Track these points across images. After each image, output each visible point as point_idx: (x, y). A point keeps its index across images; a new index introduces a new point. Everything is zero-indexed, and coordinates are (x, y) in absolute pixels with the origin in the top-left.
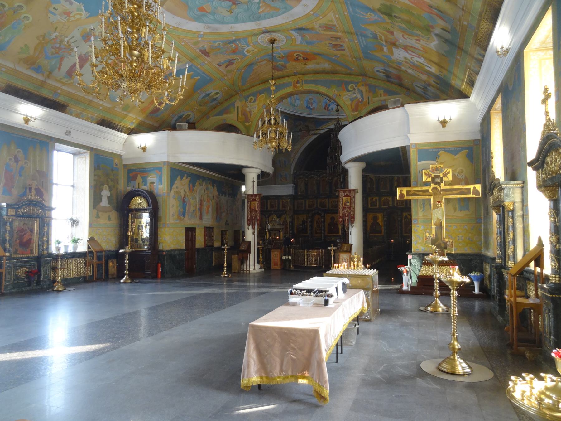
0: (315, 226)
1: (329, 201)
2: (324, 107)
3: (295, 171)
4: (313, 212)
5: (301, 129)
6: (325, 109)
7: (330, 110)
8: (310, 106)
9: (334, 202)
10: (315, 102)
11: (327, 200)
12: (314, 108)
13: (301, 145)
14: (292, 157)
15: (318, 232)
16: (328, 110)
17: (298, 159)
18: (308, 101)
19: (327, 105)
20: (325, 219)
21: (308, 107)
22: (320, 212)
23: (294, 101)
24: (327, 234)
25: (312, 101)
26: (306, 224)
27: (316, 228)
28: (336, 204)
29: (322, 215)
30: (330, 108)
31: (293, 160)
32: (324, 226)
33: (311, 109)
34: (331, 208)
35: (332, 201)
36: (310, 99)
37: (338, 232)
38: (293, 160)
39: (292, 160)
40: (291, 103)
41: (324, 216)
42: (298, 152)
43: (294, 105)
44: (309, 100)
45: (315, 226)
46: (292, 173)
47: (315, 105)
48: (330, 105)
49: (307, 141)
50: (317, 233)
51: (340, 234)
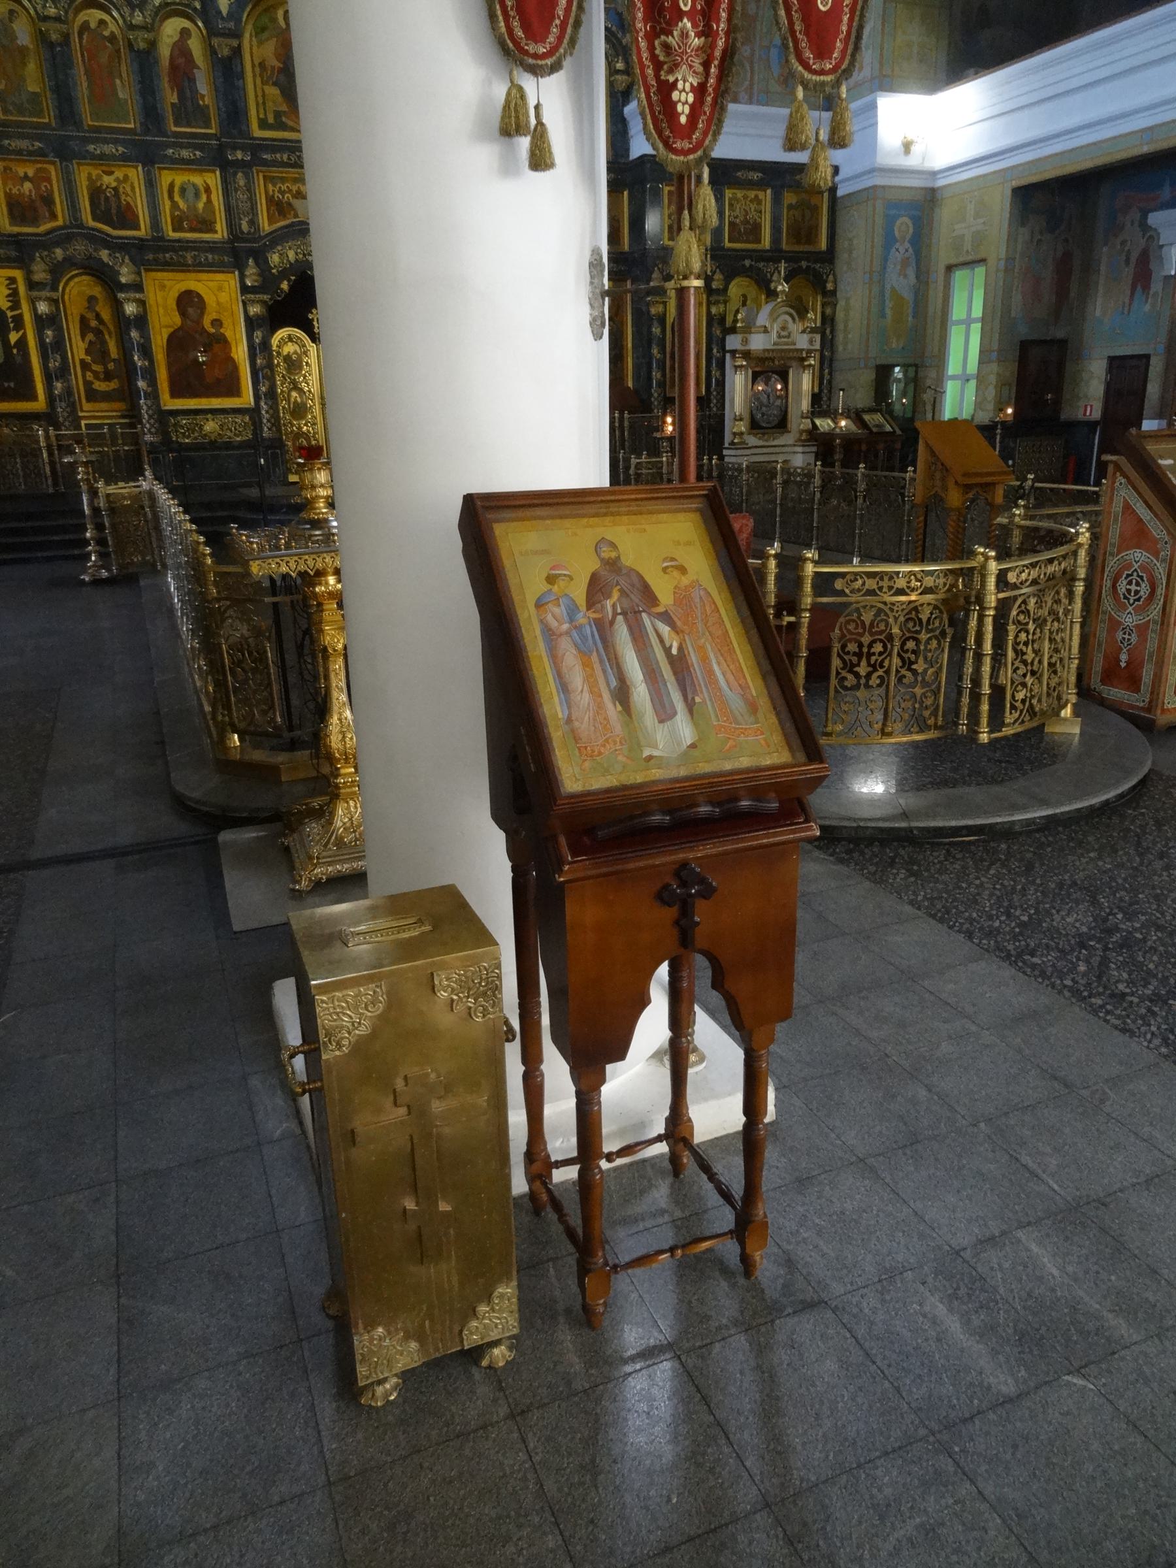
0: (78, 348)
1: (151, 184)
4: (59, 253)
9: (183, 190)
11: (135, 174)
15: (100, 386)
20: (142, 303)
22: (104, 254)
24: (171, 404)
26: (14, 337)
27: (82, 361)
28: (201, 205)
29: (126, 275)
32: (146, 352)
34: (173, 235)
35: (171, 186)
37: (233, 389)
41: (138, 287)
45: (78, 348)
50: (92, 396)
51: (247, 397)
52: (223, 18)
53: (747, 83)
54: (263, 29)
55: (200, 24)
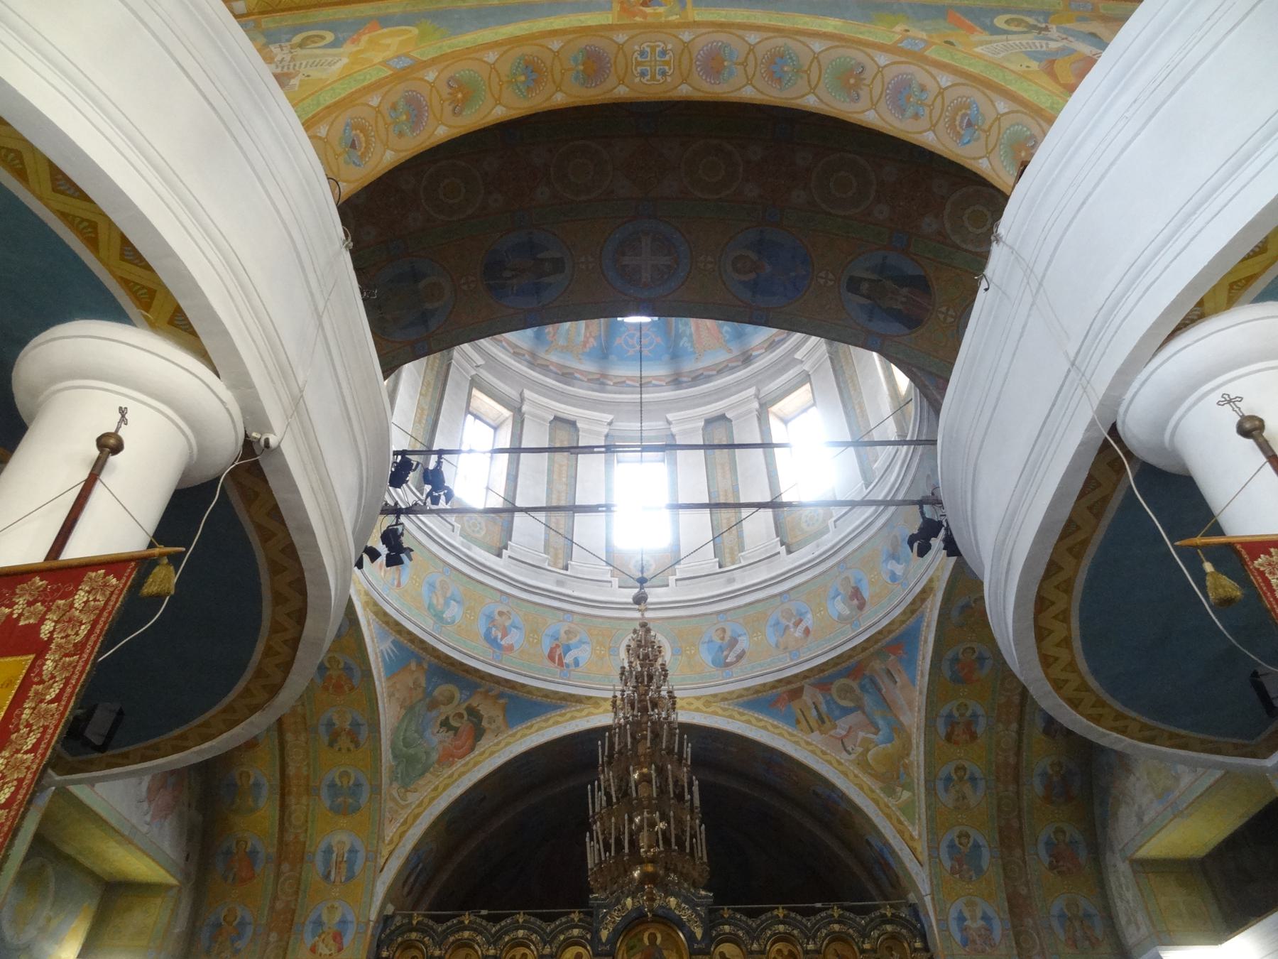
2: (546, 652)
3: (390, 909)
5: (447, 718)
6: (551, 657)
7: (568, 666)
8: (500, 637)
10: (516, 628)
12: (510, 648)
13: (436, 789)
14: (387, 839)
16: (561, 664)
17: (416, 849)
18: (490, 618)
19: (557, 646)
21: (492, 641)
23: (441, 601)
25: (507, 623)
30: (568, 659)
31: (391, 853)
33: (500, 647)
36: (501, 614)
38: (391, 853)
39: (385, 853)
40: (430, 606)
42: (416, 817)
43: (439, 617)
44: (497, 617)
46: (373, 917)
47: (514, 638)
48: (568, 649)
49: (463, 773)
52: (602, 944)
53: (1038, 947)
54: (632, 948)
55: (589, 948)
